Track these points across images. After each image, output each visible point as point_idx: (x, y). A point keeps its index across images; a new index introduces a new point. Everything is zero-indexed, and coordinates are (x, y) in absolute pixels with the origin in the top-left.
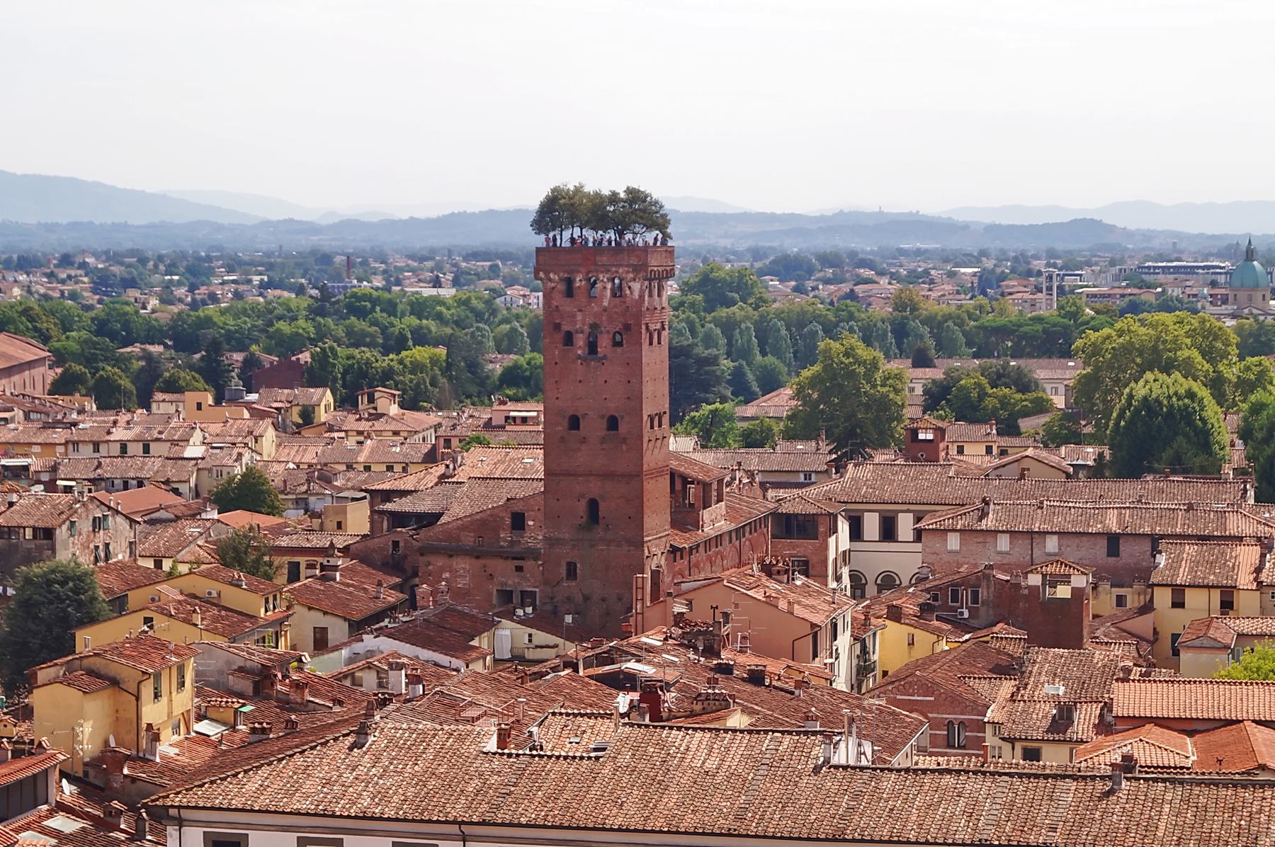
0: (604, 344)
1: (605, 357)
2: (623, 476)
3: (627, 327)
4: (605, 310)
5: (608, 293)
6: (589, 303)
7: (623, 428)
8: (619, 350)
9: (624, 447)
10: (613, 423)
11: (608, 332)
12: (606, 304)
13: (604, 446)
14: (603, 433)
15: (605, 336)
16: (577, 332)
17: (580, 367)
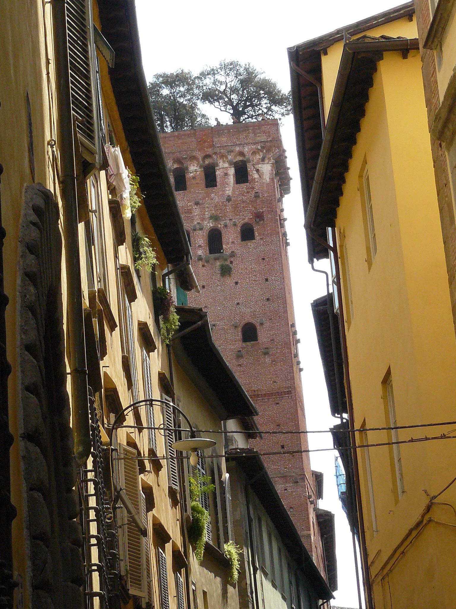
0: (231, 239)
1: (233, 254)
2: (269, 395)
3: (259, 216)
4: (229, 199)
5: (231, 179)
6: (208, 195)
7: (263, 336)
8: (251, 244)
9: (268, 360)
10: (249, 333)
11: (235, 225)
12: (229, 191)
13: (241, 360)
14: (240, 344)
15: (231, 230)
16: (195, 230)
17: (202, 271)
